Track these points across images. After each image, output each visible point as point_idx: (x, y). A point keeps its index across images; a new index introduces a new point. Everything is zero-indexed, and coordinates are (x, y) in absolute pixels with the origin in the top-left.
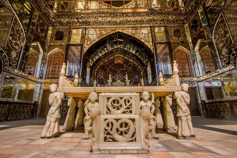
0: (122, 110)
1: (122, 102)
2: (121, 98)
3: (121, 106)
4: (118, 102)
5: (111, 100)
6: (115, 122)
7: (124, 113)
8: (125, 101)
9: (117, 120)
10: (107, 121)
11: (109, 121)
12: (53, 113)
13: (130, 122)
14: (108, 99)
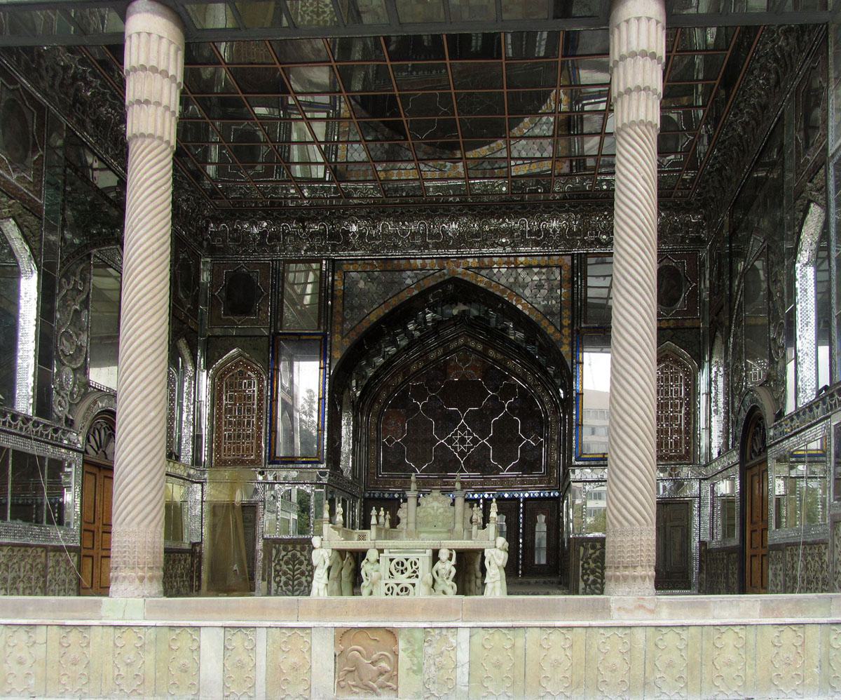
0: (407, 574)
1: (407, 564)
2: (407, 560)
3: (406, 569)
4: (403, 565)
5: (394, 562)
6: (395, 586)
7: (410, 577)
8: (411, 563)
9: (398, 585)
10: (387, 586)
11: (390, 585)
12: (321, 578)
13: (410, 587)
14: (391, 560)
